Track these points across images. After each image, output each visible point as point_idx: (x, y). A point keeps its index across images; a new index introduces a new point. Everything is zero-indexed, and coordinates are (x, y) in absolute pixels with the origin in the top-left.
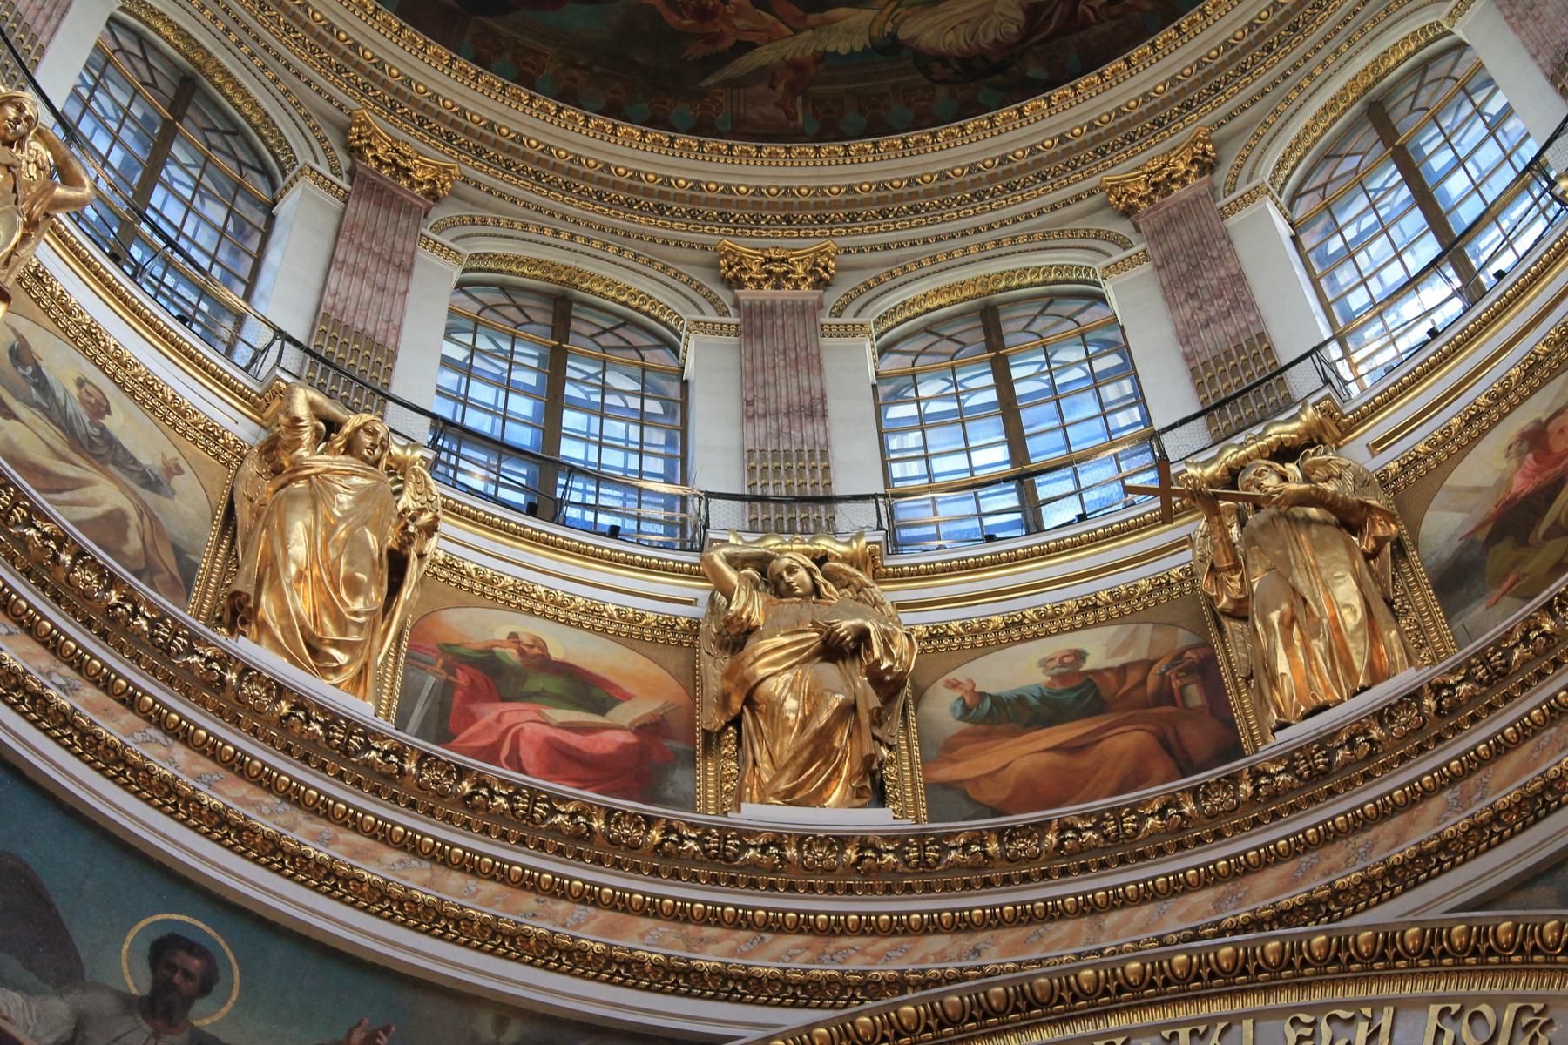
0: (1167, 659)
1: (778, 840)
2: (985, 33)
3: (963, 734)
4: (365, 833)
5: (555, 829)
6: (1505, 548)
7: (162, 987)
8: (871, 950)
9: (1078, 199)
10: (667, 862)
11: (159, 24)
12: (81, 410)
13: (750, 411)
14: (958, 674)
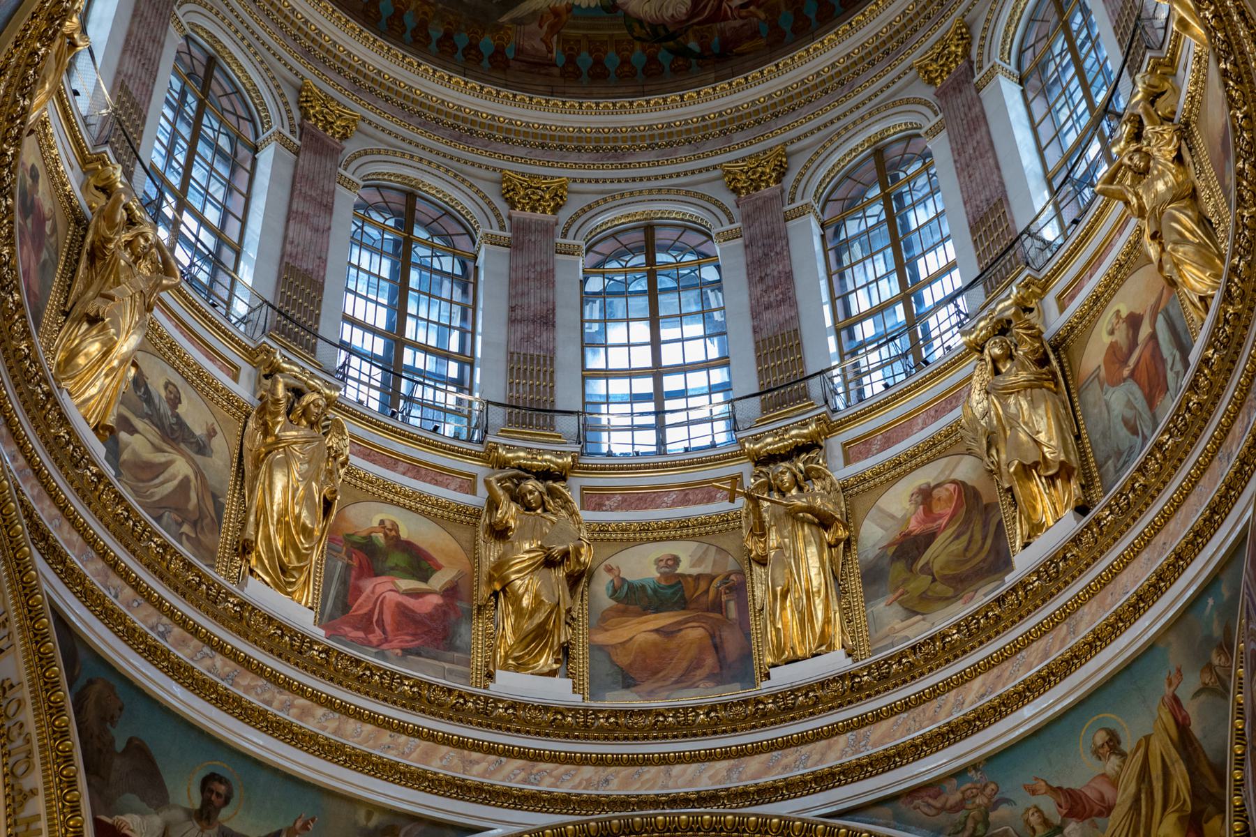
0: (721, 577)
1: (514, 705)
2: (667, 8)
3: (611, 609)
4: (307, 698)
5: (404, 692)
6: (900, 566)
7: (206, 803)
8: (555, 773)
9: (707, 169)
10: (457, 713)
11: (199, 31)
12: (167, 406)
13: (512, 321)
14: (612, 562)
